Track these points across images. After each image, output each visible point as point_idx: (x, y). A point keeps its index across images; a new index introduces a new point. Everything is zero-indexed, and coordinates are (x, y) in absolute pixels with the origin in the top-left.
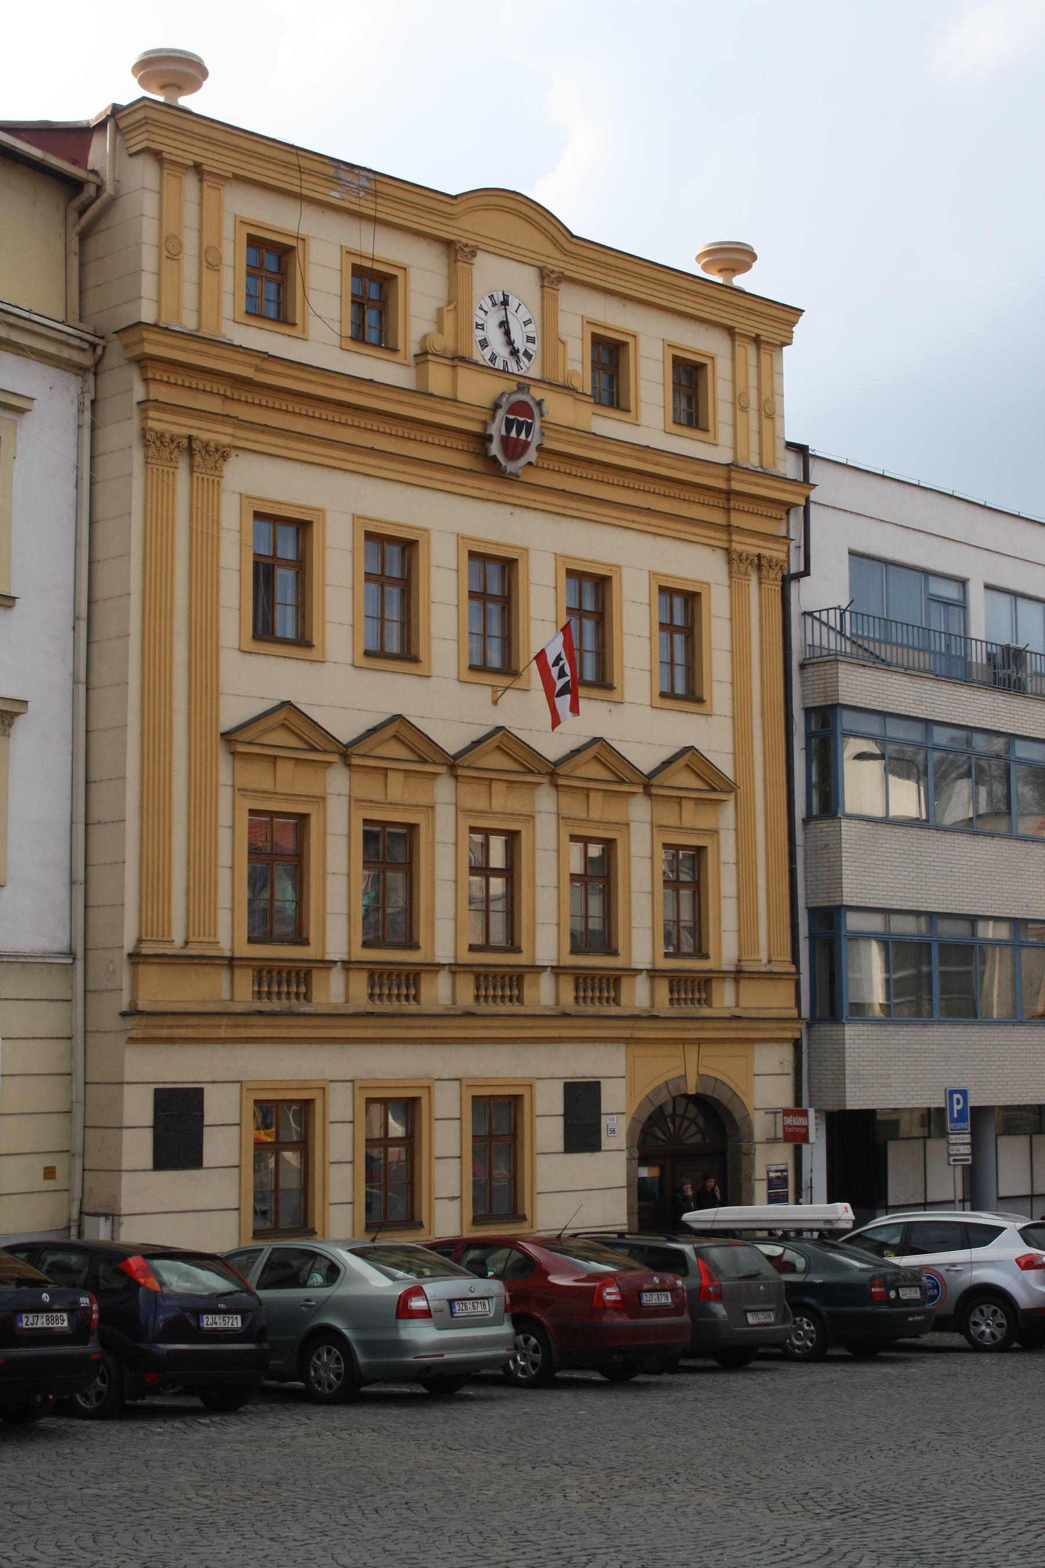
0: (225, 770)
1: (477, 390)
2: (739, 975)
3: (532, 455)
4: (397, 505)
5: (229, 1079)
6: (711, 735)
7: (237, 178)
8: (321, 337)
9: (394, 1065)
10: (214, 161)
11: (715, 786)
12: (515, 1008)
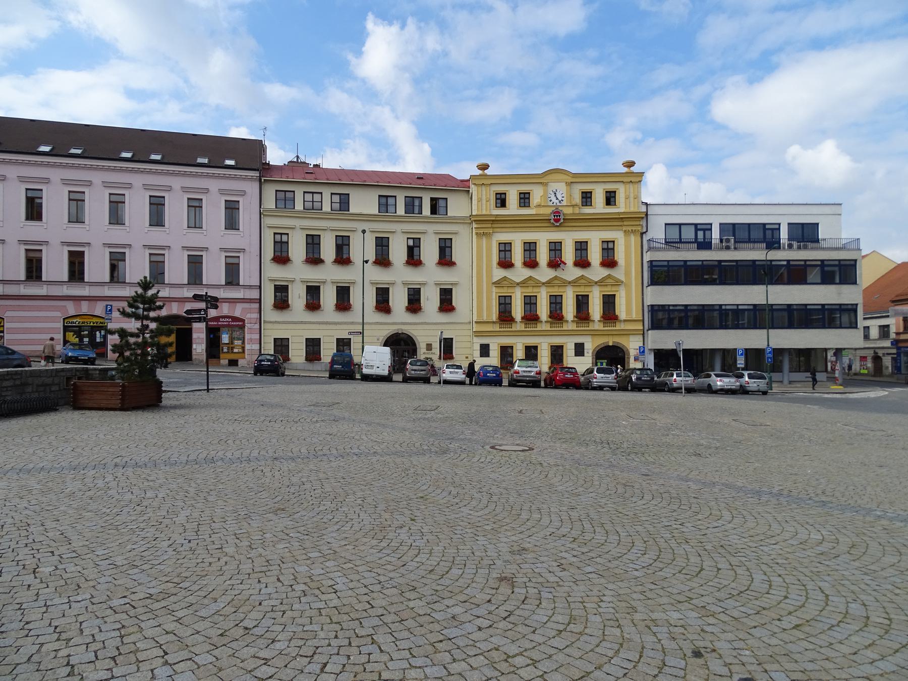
0: (494, 289)
1: (548, 211)
2: (625, 321)
4: (530, 236)
10: (486, 182)
11: (618, 283)
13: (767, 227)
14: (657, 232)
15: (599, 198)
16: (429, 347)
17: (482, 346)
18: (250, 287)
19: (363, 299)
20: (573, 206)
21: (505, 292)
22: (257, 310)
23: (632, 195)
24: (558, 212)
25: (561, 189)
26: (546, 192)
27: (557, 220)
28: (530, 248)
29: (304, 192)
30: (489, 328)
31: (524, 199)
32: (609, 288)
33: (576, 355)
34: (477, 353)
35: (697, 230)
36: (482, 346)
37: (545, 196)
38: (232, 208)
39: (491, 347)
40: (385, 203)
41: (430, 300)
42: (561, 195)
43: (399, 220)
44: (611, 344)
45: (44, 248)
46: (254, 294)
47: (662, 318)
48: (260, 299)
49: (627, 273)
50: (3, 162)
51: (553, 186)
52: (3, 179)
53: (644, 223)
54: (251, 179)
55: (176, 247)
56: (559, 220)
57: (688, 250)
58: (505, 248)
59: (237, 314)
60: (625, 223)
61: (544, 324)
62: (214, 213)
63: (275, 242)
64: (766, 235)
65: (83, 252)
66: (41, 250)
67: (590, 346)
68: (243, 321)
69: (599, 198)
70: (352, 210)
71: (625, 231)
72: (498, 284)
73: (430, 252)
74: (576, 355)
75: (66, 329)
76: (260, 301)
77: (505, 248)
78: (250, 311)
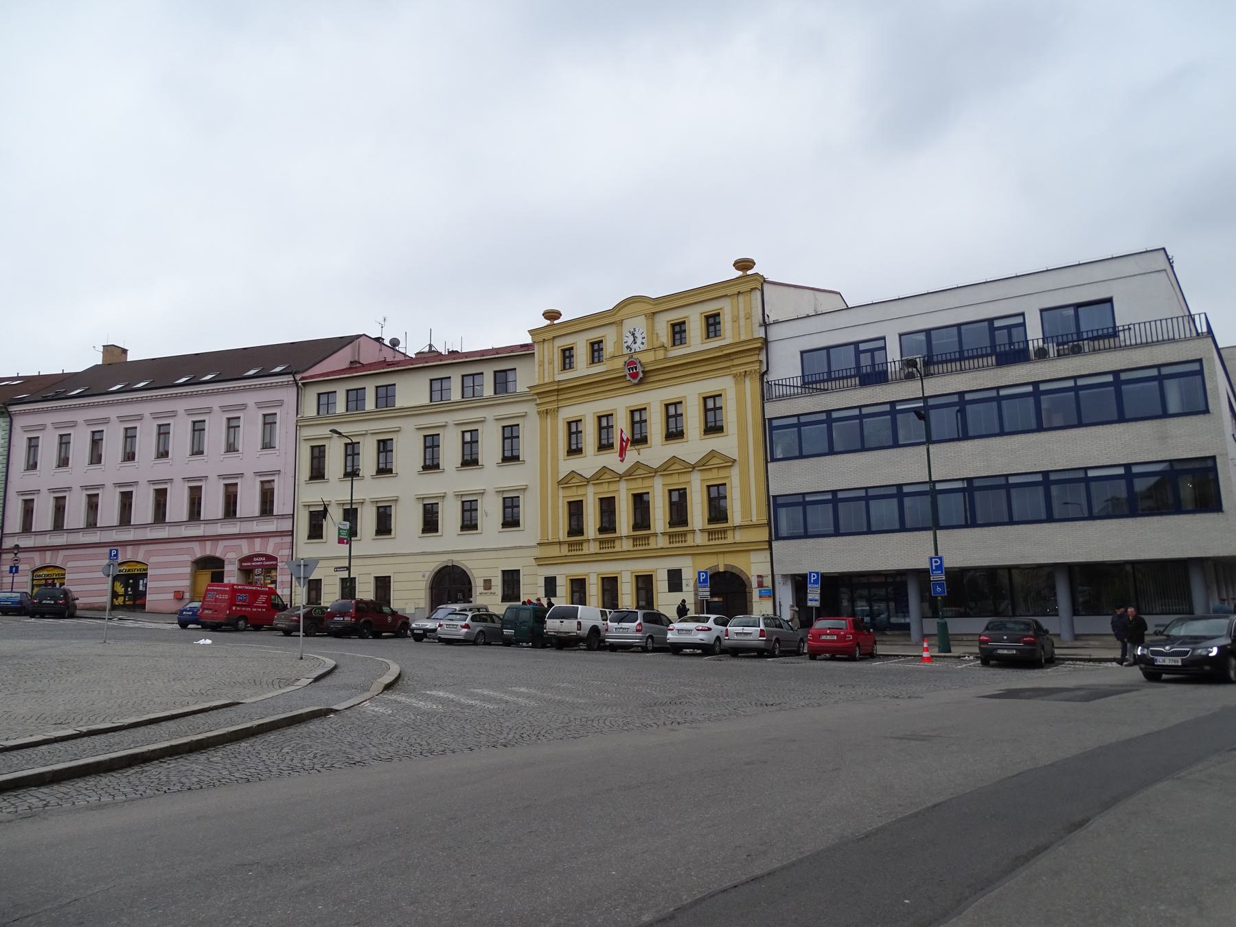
0: (561, 493)
2: (741, 527)
3: (641, 375)
4: (603, 406)
5: (593, 575)
6: (725, 444)
8: (582, 367)
9: (609, 569)
13: (997, 324)
14: (785, 366)
15: (695, 329)
16: (488, 584)
18: (283, 517)
19: (407, 519)
20: (654, 349)
22: (289, 545)
23: (742, 314)
24: (632, 363)
25: (639, 324)
26: (620, 335)
27: (638, 375)
28: (604, 423)
30: (554, 551)
31: (596, 349)
32: (714, 474)
33: (670, 591)
35: (858, 353)
38: (269, 422)
40: (438, 388)
41: (490, 513)
42: (639, 338)
43: (489, 404)
44: (721, 570)
45: (276, 478)
46: (286, 525)
47: (792, 516)
49: (743, 444)
51: (629, 325)
53: (763, 357)
54: (287, 385)
56: (637, 373)
57: (848, 388)
58: (573, 429)
59: (269, 552)
60: (736, 362)
62: (251, 433)
63: (464, 443)
64: (1000, 342)
65: (200, 487)
67: (690, 570)
68: (275, 559)
69: (695, 329)
70: (398, 405)
71: (735, 376)
72: (565, 483)
73: (490, 446)
74: (670, 591)
75: (115, 578)
77: (573, 429)
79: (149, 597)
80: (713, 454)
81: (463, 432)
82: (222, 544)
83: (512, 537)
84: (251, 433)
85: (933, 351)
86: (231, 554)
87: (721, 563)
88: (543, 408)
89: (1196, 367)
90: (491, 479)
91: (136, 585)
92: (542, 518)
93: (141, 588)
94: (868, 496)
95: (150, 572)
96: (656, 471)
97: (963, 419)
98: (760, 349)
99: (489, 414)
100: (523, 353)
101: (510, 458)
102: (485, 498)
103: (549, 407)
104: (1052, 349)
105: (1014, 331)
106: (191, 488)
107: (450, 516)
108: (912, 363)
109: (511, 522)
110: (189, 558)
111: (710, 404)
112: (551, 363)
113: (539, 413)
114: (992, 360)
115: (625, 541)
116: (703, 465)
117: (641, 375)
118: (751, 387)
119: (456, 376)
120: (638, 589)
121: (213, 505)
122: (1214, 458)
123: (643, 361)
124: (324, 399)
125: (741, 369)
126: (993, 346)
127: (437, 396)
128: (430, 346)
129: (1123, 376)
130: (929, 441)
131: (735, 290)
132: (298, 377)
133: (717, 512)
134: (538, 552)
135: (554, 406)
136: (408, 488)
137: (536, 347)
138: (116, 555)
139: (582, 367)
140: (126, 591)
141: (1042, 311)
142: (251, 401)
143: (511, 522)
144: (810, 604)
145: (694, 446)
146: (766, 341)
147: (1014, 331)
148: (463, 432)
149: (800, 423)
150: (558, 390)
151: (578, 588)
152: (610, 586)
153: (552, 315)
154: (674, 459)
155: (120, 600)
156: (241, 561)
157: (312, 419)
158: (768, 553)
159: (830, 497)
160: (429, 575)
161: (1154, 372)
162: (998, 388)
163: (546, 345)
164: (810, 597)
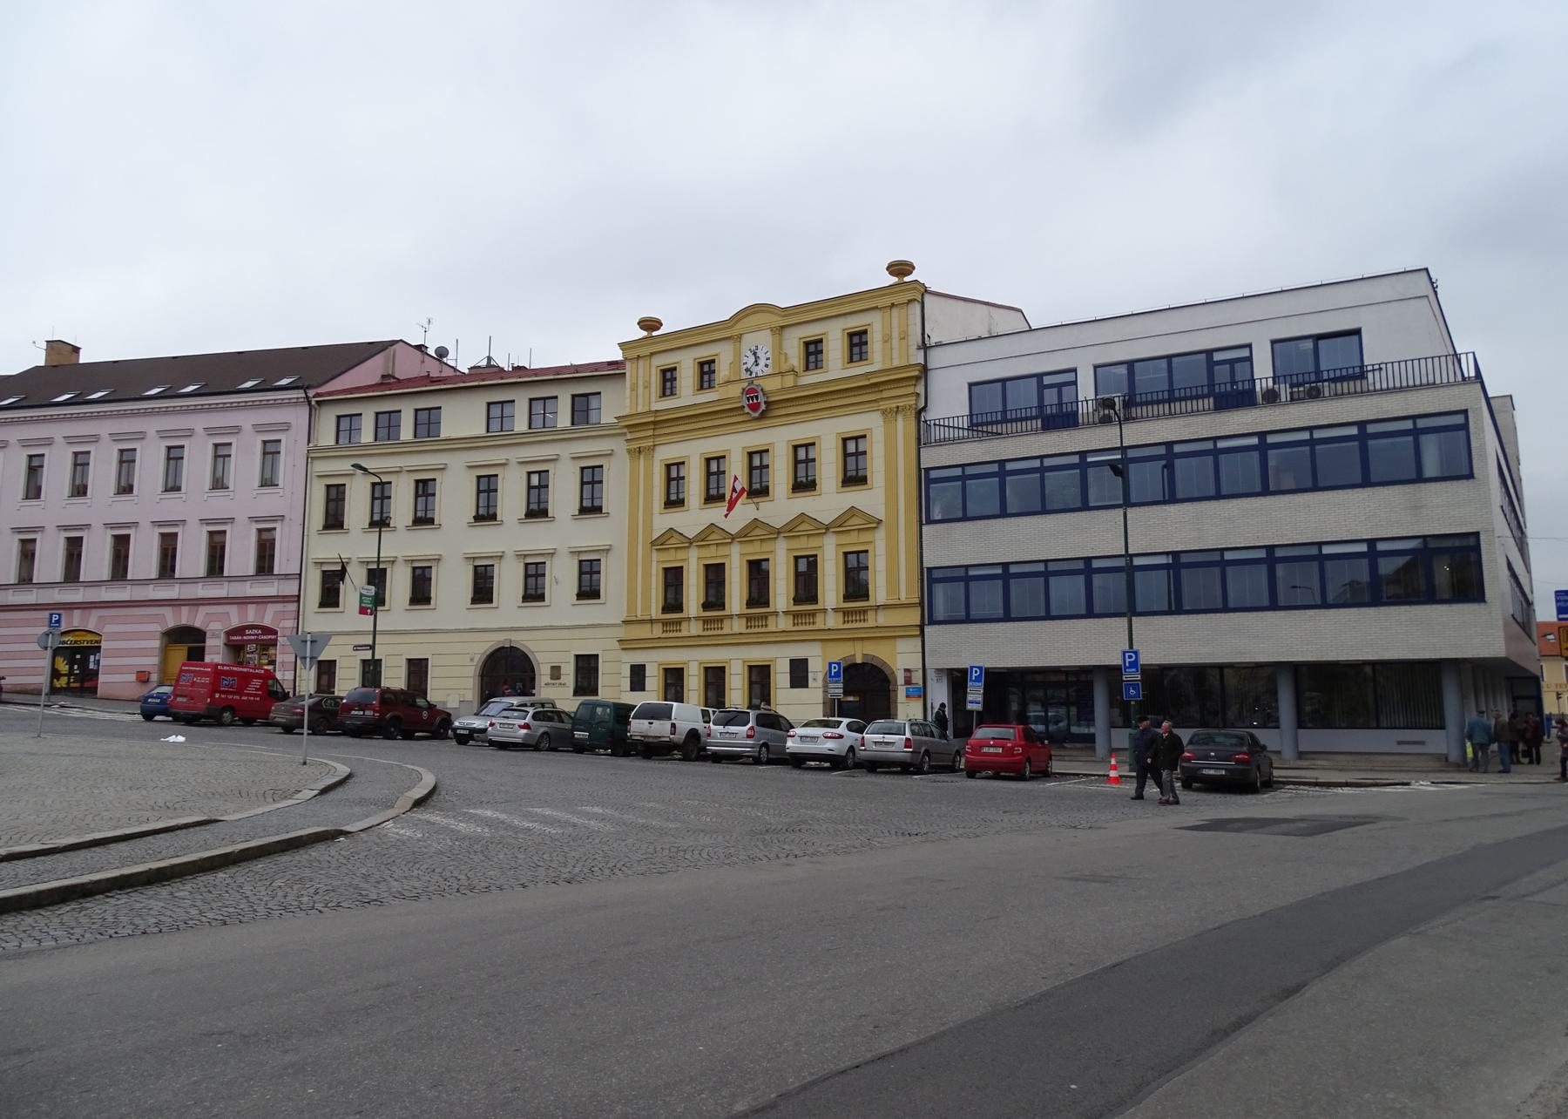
0: (655, 555)
2: (885, 607)
3: (763, 407)
4: (713, 446)
5: (694, 663)
6: (869, 500)
7: (652, 354)
9: (714, 656)
11: (874, 524)
12: (811, 627)
13: (1217, 357)
14: (949, 401)
15: (835, 350)
16: (556, 672)
17: (633, 668)
18: (287, 577)
19: (452, 585)
21: (672, 559)
22: (294, 615)
23: (895, 334)
25: (762, 341)
26: (738, 354)
28: (714, 467)
29: (489, 404)
30: (643, 632)
31: (706, 371)
32: (853, 537)
33: (792, 686)
34: (626, 684)
35: (1041, 387)
36: (633, 668)
37: (736, 363)
38: (270, 452)
39: (648, 673)
40: (497, 413)
41: (562, 579)
42: (762, 358)
43: (563, 438)
44: (859, 661)
45: (277, 525)
46: (290, 588)
47: (950, 594)
48: (299, 596)
50: (6, 422)
51: (749, 341)
52: (1, 445)
53: (920, 389)
54: (297, 403)
55: (242, 518)
57: (1027, 433)
58: (674, 474)
59: (267, 622)
60: (886, 394)
61: (693, 623)
62: (245, 464)
63: (530, 487)
64: (1219, 380)
66: (224, 532)
67: (818, 661)
68: (275, 632)
69: (835, 350)
70: (443, 435)
71: (884, 412)
73: (564, 493)
74: (792, 686)
75: (57, 652)
76: (297, 599)
77: (674, 474)
78: (280, 616)
79: (102, 678)
80: (853, 511)
81: (529, 474)
82: (203, 610)
83: (589, 612)
84: (245, 464)
85: (1136, 388)
86: (216, 626)
87: (858, 653)
88: (635, 445)
89: (1459, 419)
90: (564, 536)
91: (85, 661)
92: (629, 587)
93: (91, 666)
94: (1047, 571)
95: (104, 645)
96: (779, 532)
97: (1172, 476)
98: (917, 378)
99: (565, 450)
100: (611, 372)
101: (591, 509)
102: (556, 560)
103: (643, 444)
104: (1284, 391)
105: (1238, 366)
106: (163, 535)
107: (508, 582)
108: (1109, 404)
109: (589, 591)
110: (158, 628)
111: (851, 447)
112: (647, 387)
113: (629, 451)
114: (1209, 403)
115: (736, 622)
116: (838, 526)
117: (763, 407)
118: (904, 427)
119: (521, 400)
120: (751, 683)
121: (192, 558)
122: (1477, 534)
123: (767, 389)
124: (345, 424)
125: (893, 404)
126: (1211, 385)
127: (495, 425)
128: (489, 358)
129: (1371, 429)
130: (1127, 503)
131: (887, 301)
132: (311, 393)
133: (856, 587)
134: (623, 633)
135: (649, 443)
136: (454, 543)
137: (628, 365)
138: (58, 622)
139: (687, 393)
140: (71, 668)
141: (1273, 342)
142: (247, 422)
143: (589, 591)
144: (970, 707)
145: (829, 501)
146: (925, 369)
147: (1238, 366)
148: (529, 474)
149: (964, 475)
150: (654, 423)
151: (674, 680)
152: (715, 678)
153: (649, 324)
154: (802, 517)
155: (63, 682)
156: (229, 633)
157: (329, 448)
158: (918, 641)
159: (999, 571)
160: (479, 659)
161: (1408, 425)
162: (1215, 439)
163: (641, 363)
164: (970, 698)
